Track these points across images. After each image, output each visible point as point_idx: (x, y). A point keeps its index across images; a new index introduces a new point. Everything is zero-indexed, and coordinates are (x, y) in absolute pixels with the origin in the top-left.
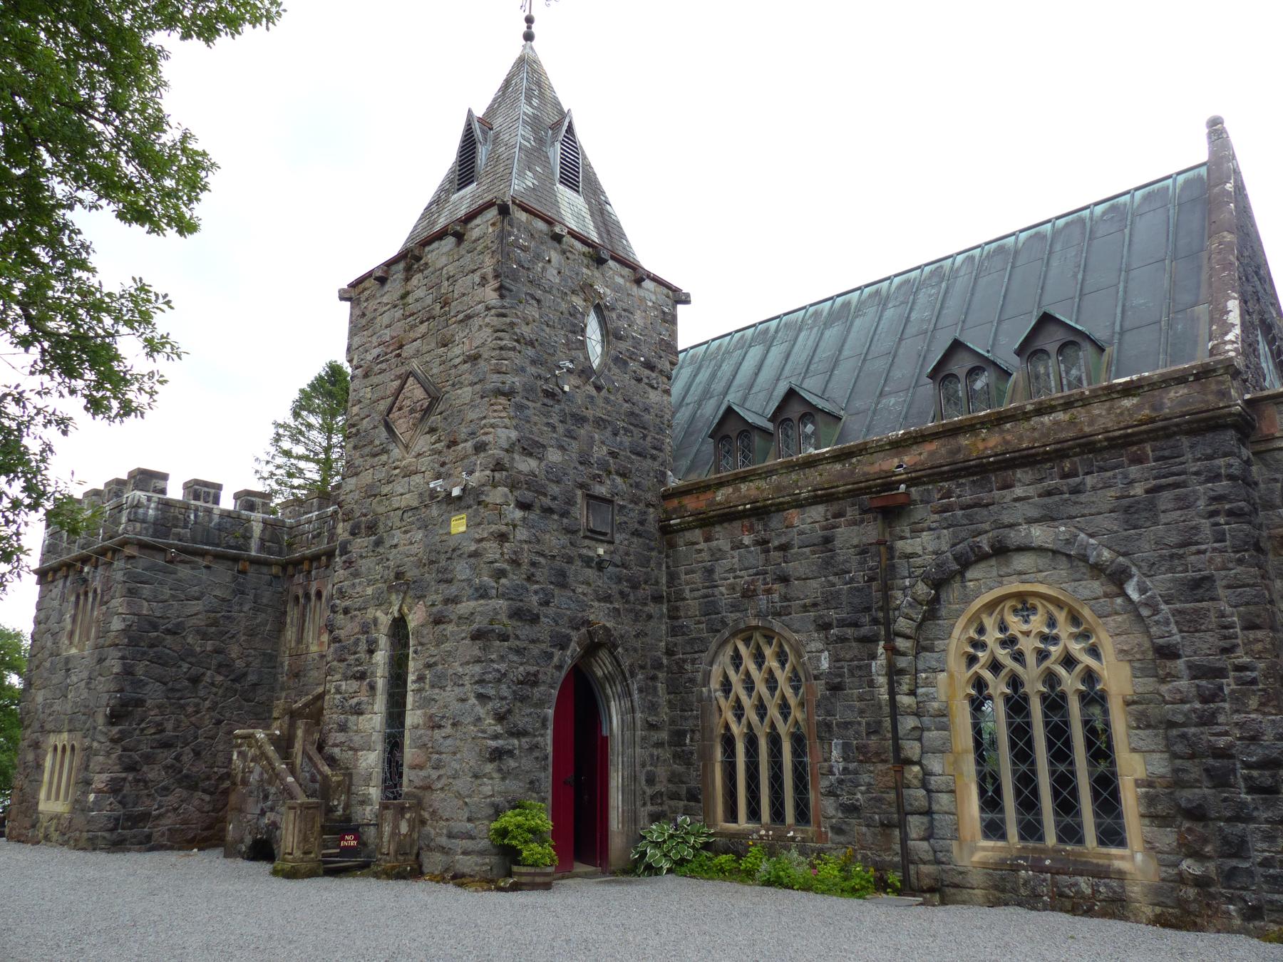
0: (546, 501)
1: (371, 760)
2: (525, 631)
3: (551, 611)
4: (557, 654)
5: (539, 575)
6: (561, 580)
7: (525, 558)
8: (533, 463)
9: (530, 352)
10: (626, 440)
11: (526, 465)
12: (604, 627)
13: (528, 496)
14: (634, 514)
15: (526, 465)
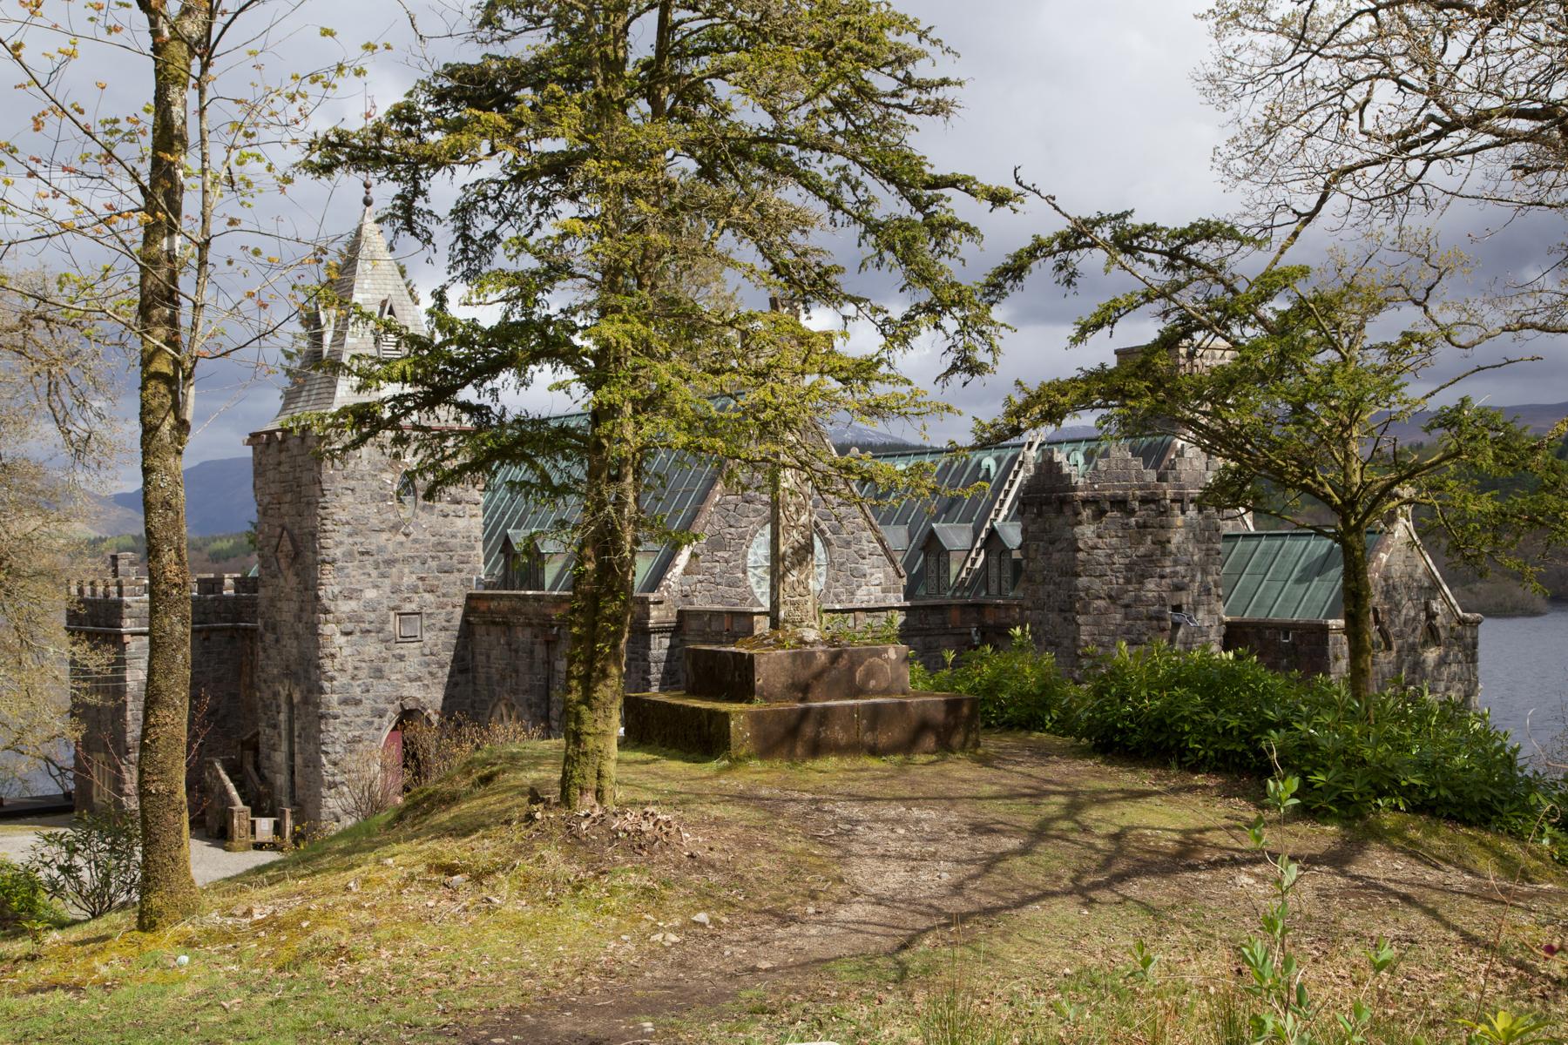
0: (366, 626)
1: (281, 780)
2: (350, 710)
3: (371, 695)
4: (376, 720)
5: (361, 674)
6: (378, 674)
7: (349, 667)
8: (353, 604)
9: (347, 528)
10: (434, 564)
11: (345, 607)
12: (417, 700)
13: (349, 626)
14: (443, 617)
15: (345, 607)
